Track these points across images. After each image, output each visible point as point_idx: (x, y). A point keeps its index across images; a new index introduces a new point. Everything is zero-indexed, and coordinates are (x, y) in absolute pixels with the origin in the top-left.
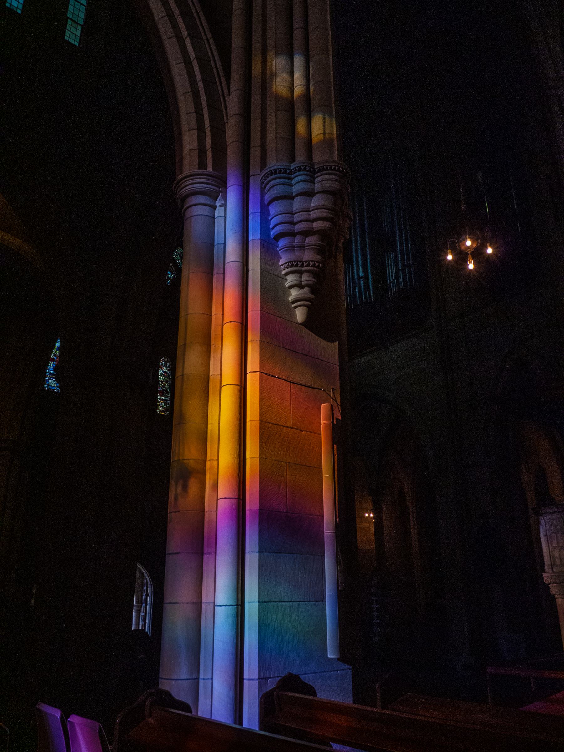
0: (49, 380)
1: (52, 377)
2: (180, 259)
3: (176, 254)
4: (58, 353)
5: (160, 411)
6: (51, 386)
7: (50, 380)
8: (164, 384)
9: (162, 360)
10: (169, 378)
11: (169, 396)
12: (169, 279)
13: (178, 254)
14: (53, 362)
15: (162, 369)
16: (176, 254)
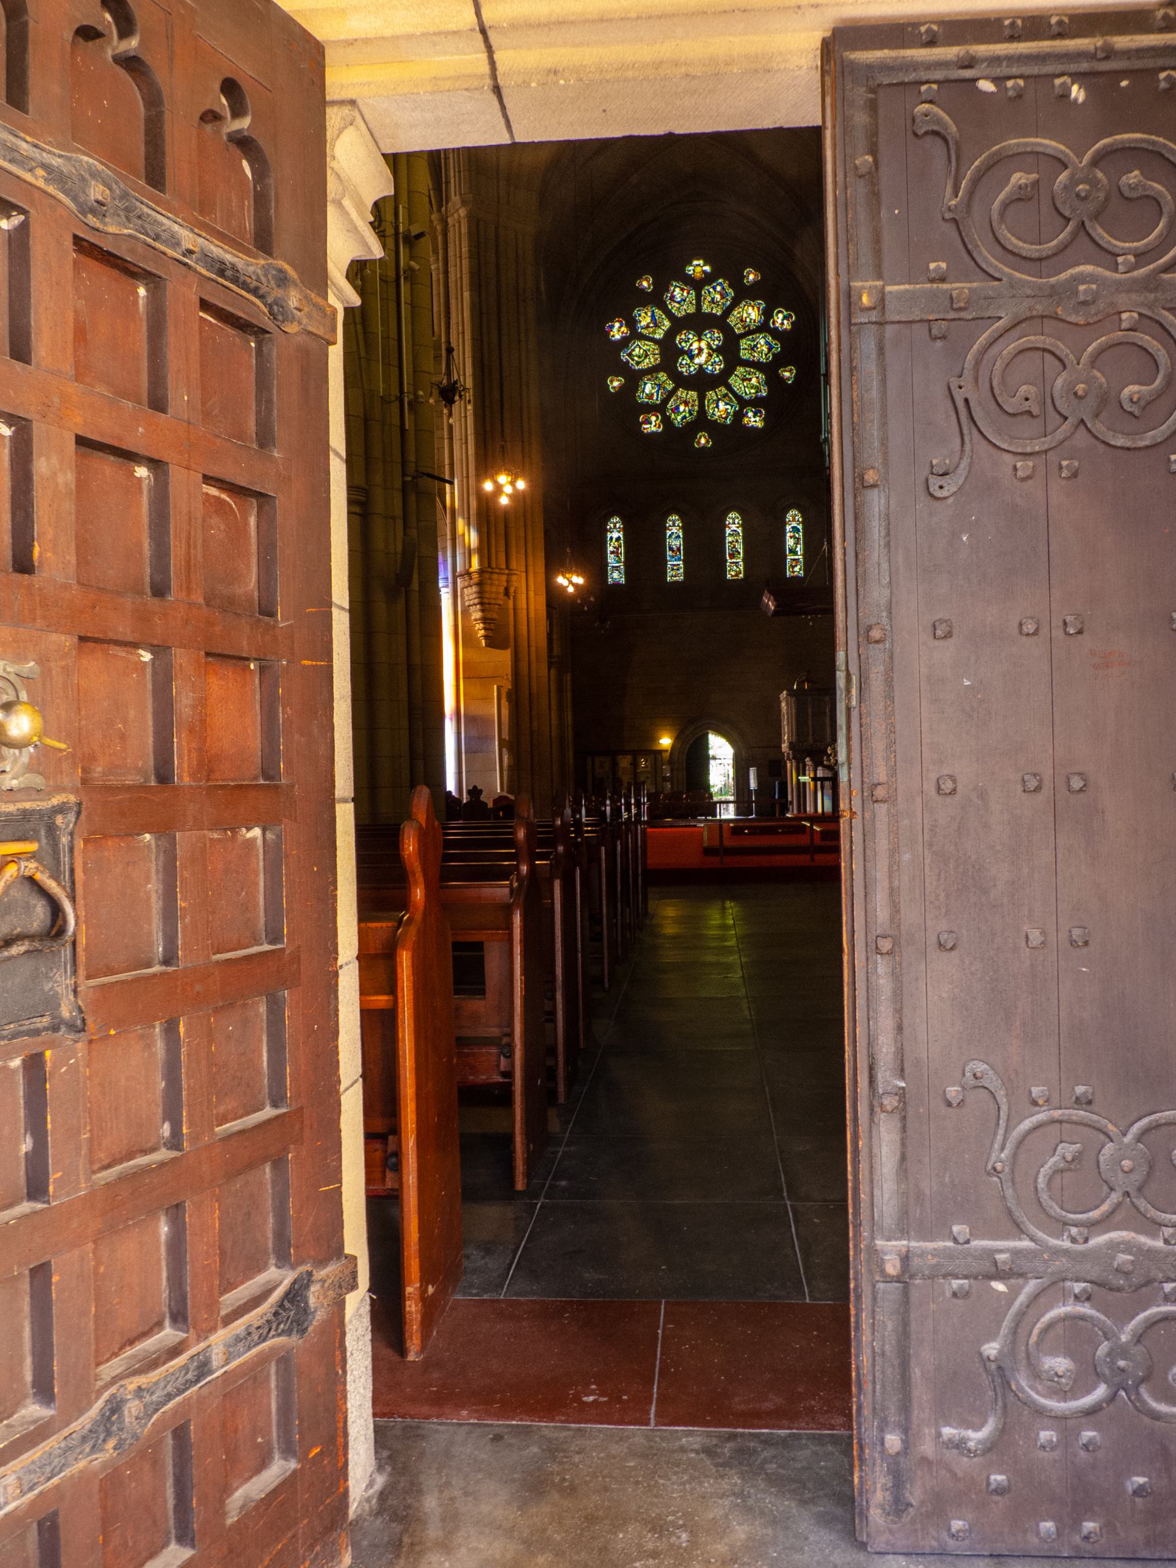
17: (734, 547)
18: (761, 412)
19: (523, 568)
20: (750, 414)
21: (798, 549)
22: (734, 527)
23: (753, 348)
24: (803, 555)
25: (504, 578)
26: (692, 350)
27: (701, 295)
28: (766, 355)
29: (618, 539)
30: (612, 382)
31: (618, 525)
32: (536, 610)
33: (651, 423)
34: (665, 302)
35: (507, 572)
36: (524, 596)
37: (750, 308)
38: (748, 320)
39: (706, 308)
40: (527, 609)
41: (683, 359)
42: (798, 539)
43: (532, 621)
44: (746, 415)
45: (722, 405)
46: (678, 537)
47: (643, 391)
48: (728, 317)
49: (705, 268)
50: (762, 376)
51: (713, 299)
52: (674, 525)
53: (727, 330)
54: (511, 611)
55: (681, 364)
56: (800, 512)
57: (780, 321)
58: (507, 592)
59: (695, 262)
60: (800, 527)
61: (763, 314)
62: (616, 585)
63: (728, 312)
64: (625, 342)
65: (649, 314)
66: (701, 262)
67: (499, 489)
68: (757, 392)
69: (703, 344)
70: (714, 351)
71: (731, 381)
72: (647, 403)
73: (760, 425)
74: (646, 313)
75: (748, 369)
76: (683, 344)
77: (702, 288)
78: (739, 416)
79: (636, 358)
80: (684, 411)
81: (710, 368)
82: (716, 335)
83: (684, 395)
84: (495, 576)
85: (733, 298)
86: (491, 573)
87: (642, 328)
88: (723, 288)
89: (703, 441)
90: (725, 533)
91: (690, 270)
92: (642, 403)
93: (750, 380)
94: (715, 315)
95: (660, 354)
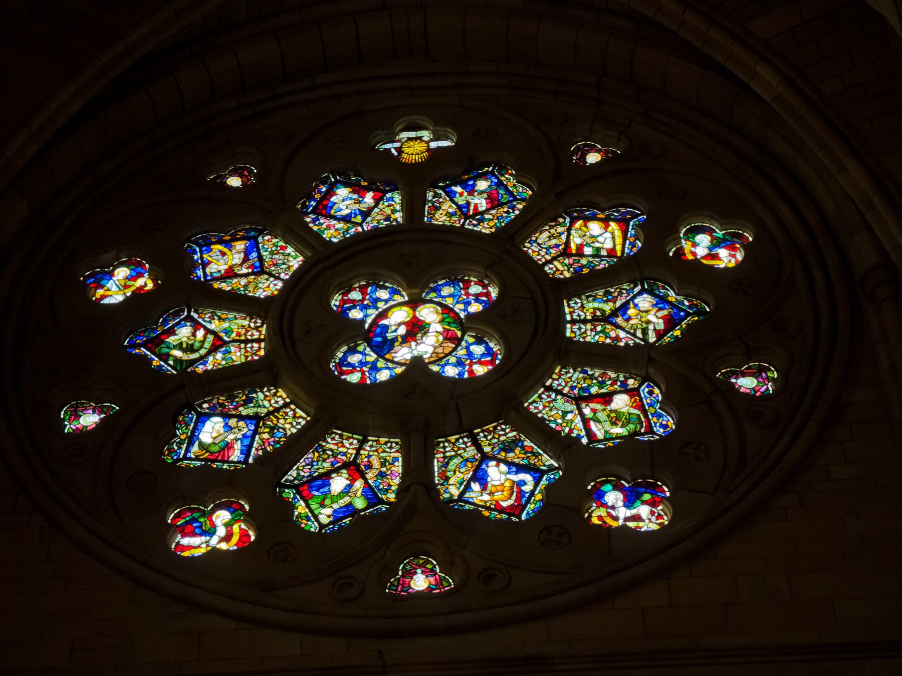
12: (528, 502)
13: (559, 392)
16: (549, 396)
20: (613, 497)
26: (386, 328)
38: (588, 251)
41: (353, 351)
44: (599, 496)
45: (496, 473)
55: (343, 362)
59: (404, 135)
75: (597, 373)
79: (177, 353)
80: (346, 491)
93: (606, 399)
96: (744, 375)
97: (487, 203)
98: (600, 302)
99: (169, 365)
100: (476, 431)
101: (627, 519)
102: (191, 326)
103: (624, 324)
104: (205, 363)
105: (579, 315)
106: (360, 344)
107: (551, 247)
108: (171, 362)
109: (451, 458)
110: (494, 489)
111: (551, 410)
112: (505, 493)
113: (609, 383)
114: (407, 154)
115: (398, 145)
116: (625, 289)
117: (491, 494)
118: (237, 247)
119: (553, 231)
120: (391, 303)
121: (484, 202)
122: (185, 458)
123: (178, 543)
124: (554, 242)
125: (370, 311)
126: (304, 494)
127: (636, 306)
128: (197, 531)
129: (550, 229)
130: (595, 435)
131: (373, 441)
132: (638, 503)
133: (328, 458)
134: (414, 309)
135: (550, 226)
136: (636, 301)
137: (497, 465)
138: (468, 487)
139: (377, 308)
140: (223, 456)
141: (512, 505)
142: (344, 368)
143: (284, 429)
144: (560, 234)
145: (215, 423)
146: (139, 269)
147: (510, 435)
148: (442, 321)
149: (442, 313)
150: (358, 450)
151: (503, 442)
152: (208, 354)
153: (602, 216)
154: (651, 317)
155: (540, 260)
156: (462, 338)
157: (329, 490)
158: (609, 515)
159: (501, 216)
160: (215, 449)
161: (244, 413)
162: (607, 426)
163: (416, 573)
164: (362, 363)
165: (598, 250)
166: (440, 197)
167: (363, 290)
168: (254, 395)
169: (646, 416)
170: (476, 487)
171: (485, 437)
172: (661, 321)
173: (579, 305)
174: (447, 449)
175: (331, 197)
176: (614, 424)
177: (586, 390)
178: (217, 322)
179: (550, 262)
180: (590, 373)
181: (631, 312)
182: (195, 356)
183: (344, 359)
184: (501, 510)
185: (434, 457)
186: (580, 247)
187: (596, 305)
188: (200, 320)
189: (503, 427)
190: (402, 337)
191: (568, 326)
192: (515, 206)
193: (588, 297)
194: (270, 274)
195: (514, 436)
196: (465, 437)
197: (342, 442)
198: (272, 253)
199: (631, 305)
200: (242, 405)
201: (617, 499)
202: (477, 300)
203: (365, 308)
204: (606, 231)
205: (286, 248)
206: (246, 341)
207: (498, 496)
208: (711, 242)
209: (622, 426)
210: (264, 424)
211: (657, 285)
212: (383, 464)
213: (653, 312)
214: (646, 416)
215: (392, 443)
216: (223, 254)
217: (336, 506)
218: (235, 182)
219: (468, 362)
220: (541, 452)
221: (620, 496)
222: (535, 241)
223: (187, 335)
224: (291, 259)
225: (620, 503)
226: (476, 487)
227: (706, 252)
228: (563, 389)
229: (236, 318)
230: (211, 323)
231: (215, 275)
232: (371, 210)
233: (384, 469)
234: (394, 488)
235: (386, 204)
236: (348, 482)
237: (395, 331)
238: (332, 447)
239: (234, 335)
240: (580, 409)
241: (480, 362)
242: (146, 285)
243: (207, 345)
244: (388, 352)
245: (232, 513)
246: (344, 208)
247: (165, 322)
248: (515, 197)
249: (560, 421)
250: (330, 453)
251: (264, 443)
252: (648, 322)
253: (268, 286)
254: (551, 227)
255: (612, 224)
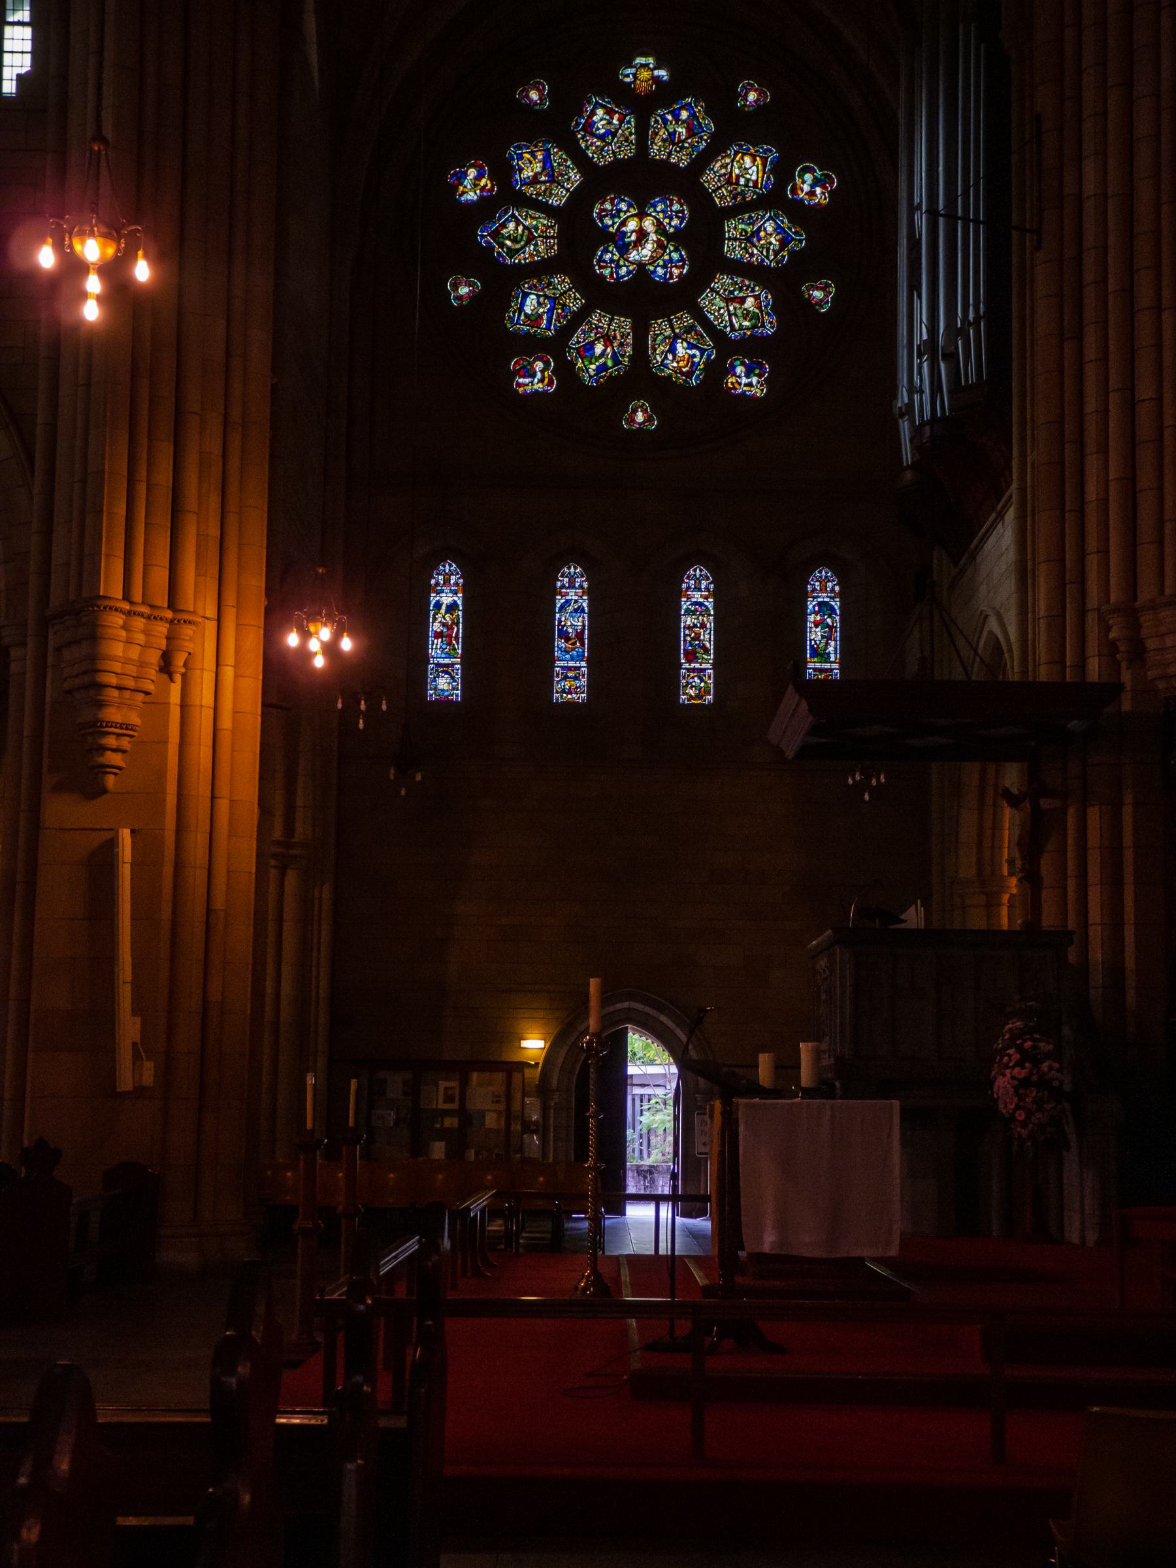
0: (437, 679)
1: (441, 672)
2: (723, 305)
3: (712, 295)
4: (448, 619)
5: (691, 697)
6: (443, 690)
7: (438, 678)
8: (696, 634)
9: (688, 578)
10: (709, 615)
11: (710, 659)
12: (696, 369)
13: (717, 293)
14: (440, 640)
15: (688, 598)
16: (712, 295)
17: (697, 637)
18: (761, 366)
19: (211, 612)
20: (739, 370)
21: (831, 649)
22: (697, 597)
23: (749, 239)
24: (842, 662)
25: (162, 629)
26: (625, 233)
27: (648, 126)
28: (776, 253)
29: (452, 608)
30: (455, 287)
31: (453, 579)
32: (235, 712)
33: (533, 375)
34: (574, 134)
35: (169, 614)
36: (208, 678)
37: (747, 160)
38: (742, 181)
39: (657, 149)
40: (216, 709)
41: (606, 251)
42: (831, 627)
43: (225, 739)
46: (580, 610)
47: (521, 309)
48: (702, 172)
49: (656, 73)
50: (766, 296)
51: (672, 135)
52: (572, 586)
53: (699, 199)
54: (175, 712)
55: (601, 260)
56: (835, 573)
57: (806, 188)
58: (166, 666)
59: (640, 60)
60: (836, 604)
61: (771, 171)
62: (444, 703)
63: (702, 161)
64: (487, 208)
65: (540, 156)
66: (651, 60)
67: (74, 268)
68: (754, 327)
69: (648, 225)
70: (670, 238)
71: (704, 301)
72: (528, 333)
73: (758, 391)
74: (533, 154)
76: (608, 221)
77: (651, 112)
78: (717, 371)
79: (508, 243)
80: (603, 354)
81: (660, 271)
82: (676, 207)
83: (604, 323)
84: (139, 623)
85: (713, 136)
86: (129, 613)
87: (524, 183)
88: (693, 115)
89: (640, 417)
90: (680, 608)
91: (627, 75)
92: (515, 334)
93: (742, 301)
94: (676, 165)
95: (560, 237)
96: (818, 289)
97: (686, 133)
98: (745, 224)
99: (504, 252)
100: (672, 317)
101: (746, 385)
102: (514, 221)
103: (757, 244)
104: (524, 253)
105: (733, 234)
106: (610, 246)
107: (721, 176)
108: (505, 249)
109: (658, 335)
110: (679, 359)
111: (712, 305)
112: (685, 362)
113: (745, 288)
114: (640, 80)
115: (633, 70)
116: (760, 215)
117: (678, 362)
118: (539, 157)
119: (723, 161)
120: (629, 214)
121: (684, 130)
122: (518, 323)
123: (517, 381)
124: (723, 171)
125: (616, 220)
126: (582, 353)
127: (765, 230)
128: (527, 374)
129: (722, 159)
130: (734, 325)
131: (617, 319)
132: (752, 375)
133: (593, 330)
134: (641, 220)
135: (722, 156)
136: (766, 225)
137: (682, 343)
138: (666, 357)
139: (620, 218)
140: (538, 324)
141: (688, 371)
142: (602, 264)
143: (569, 306)
144: (728, 164)
145: (533, 299)
146: (482, 171)
147: (690, 322)
148: (656, 232)
149: (657, 225)
150: (609, 325)
151: (686, 327)
152: (525, 245)
153: (752, 151)
154: (773, 240)
155: (714, 186)
156: (667, 247)
157: (594, 353)
158: (737, 381)
159: (694, 145)
160: (533, 318)
161: (547, 293)
162: (741, 319)
163: (638, 411)
164: (612, 261)
165: (748, 180)
166: (658, 124)
167: (612, 201)
168: (552, 280)
169: (762, 315)
170: (670, 357)
171: (677, 322)
172: (778, 243)
173: (734, 225)
174: (657, 329)
175: (593, 116)
176: (745, 319)
177: (732, 292)
178: (529, 220)
179: (719, 188)
180: (735, 280)
181: (762, 234)
182: (518, 246)
183: (601, 256)
184: (683, 374)
185: (649, 334)
186: (738, 177)
187: (743, 226)
188: (519, 217)
189: (686, 315)
190: (634, 242)
191: (726, 242)
192: (702, 136)
193: (739, 219)
194: (559, 184)
195: (692, 323)
196: (666, 321)
197: (600, 319)
198: (559, 165)
199: (763, 229)
200: (546, 287)
201: (741, 371)
202: (677, 217)
203: (613, 217)
204: (754, 165)
205: (566, 161)
206: (547, 237)
207: (681, 364)
208: (813, 180)
209: (749, 321)
210: (559, 302)
211: (778, 213)
212: (622, 337)
213: (774, 236)
214: (762, 315)
215: (627, 321)
216: (531, 162)
217: (597, 364)
218: (534, 95)
219: (669, 265)
220: (705, 335)
221: (744, 370)
222: (713, 169)
223: (513, 229)
224: (570, 171)
225: (743, 375)
226: (670, 357)
227: (809, 189)
228: (720, 291)
229: (539, 217)
230: (525, 220)
231: (527, 180)
232: (617, 131)
233: (623, 340)
234: (627, 354)
235: (626, 126)
236: (604, 348)
237: (630, 237)
238: (595, 322)
239: (539, 231)
240: (727, 306)
241: (677, 267)
242: (486, 185)
243: (524, 239)
244: (626, 253)
245: (544, 364)
246: (601, 127)
247: (500, 218)
248: (702, 128)
249: (716, 314)
250: (594, 326)
251: (559, 316)
252: (771, 243)
253: (558, 193)
254: (723, 158)
255: (758, 158)
